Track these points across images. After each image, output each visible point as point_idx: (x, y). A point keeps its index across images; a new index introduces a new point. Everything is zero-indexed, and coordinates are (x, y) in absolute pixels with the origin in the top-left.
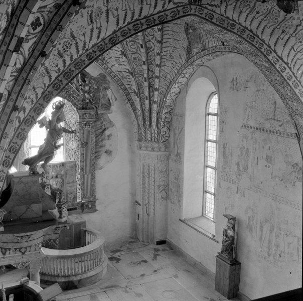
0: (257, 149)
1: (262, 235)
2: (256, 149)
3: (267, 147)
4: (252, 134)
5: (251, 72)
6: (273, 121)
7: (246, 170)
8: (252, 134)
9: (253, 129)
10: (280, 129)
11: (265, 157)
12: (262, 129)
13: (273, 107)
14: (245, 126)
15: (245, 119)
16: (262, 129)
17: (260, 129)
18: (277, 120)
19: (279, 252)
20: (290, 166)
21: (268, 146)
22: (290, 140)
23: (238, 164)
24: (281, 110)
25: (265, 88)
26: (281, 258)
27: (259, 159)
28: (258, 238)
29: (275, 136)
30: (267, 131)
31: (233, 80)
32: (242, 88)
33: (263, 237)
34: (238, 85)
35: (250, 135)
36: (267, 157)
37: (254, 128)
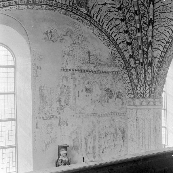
0: (77, 85)
1: (87, 147)
2: (76, 85)
3: (86, 82)
4: (72, 75)
5: (66, 29)
6: (89, 64)
7: (67, 104)
8: (72, 75)
9: (72, 71)
10: (95, 69)
11: (84, 89)
12: (80, 70)
13: (87, 55)
14: (64, 70)
15: (63, 64)
16: (80, 70)
17: (79, 70)
18: (92, 63)
19: (101, 151)
20: (104, 91)
21: (87, 81)
22: (102, 75)
23: (59, 101)
24: (94, 56)
25: (80, 42)
26: (104, 154)
27: (79, 93)
28: (84, 151)
29: (92, 74)
30: (84, 71)
31: (47, 32)
32: (59, 40)
33: (88, 147)
34: (53, 38)
35: (70, 76)
36: (87, 89)
37: (73, 70)
